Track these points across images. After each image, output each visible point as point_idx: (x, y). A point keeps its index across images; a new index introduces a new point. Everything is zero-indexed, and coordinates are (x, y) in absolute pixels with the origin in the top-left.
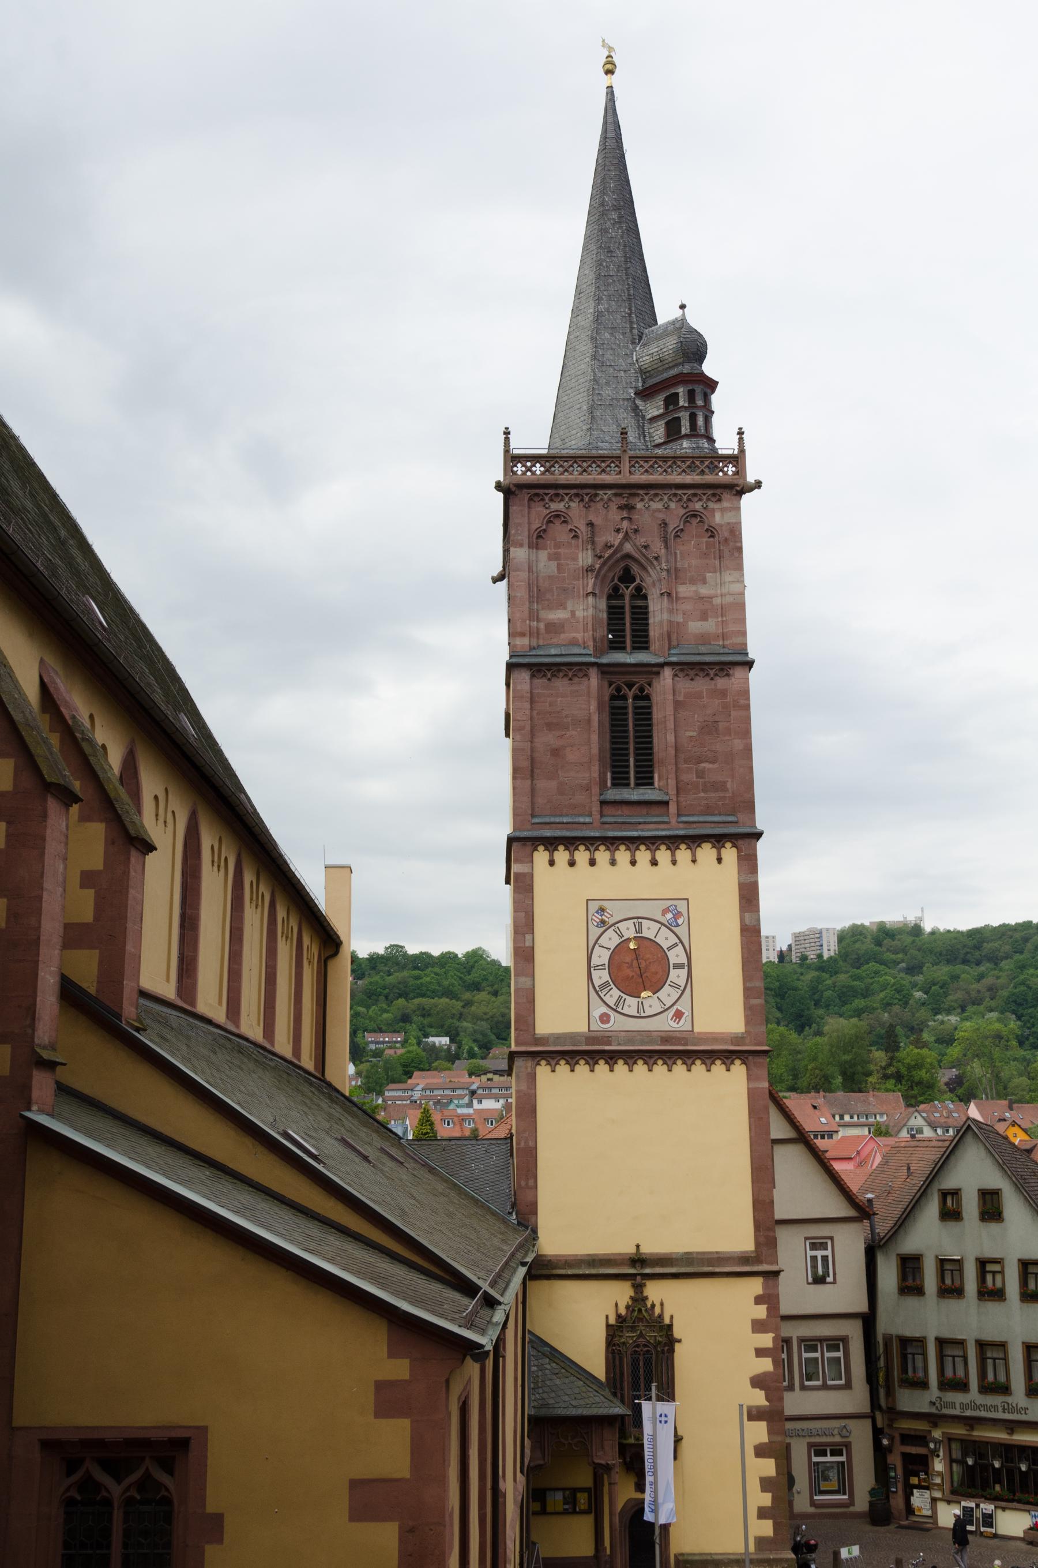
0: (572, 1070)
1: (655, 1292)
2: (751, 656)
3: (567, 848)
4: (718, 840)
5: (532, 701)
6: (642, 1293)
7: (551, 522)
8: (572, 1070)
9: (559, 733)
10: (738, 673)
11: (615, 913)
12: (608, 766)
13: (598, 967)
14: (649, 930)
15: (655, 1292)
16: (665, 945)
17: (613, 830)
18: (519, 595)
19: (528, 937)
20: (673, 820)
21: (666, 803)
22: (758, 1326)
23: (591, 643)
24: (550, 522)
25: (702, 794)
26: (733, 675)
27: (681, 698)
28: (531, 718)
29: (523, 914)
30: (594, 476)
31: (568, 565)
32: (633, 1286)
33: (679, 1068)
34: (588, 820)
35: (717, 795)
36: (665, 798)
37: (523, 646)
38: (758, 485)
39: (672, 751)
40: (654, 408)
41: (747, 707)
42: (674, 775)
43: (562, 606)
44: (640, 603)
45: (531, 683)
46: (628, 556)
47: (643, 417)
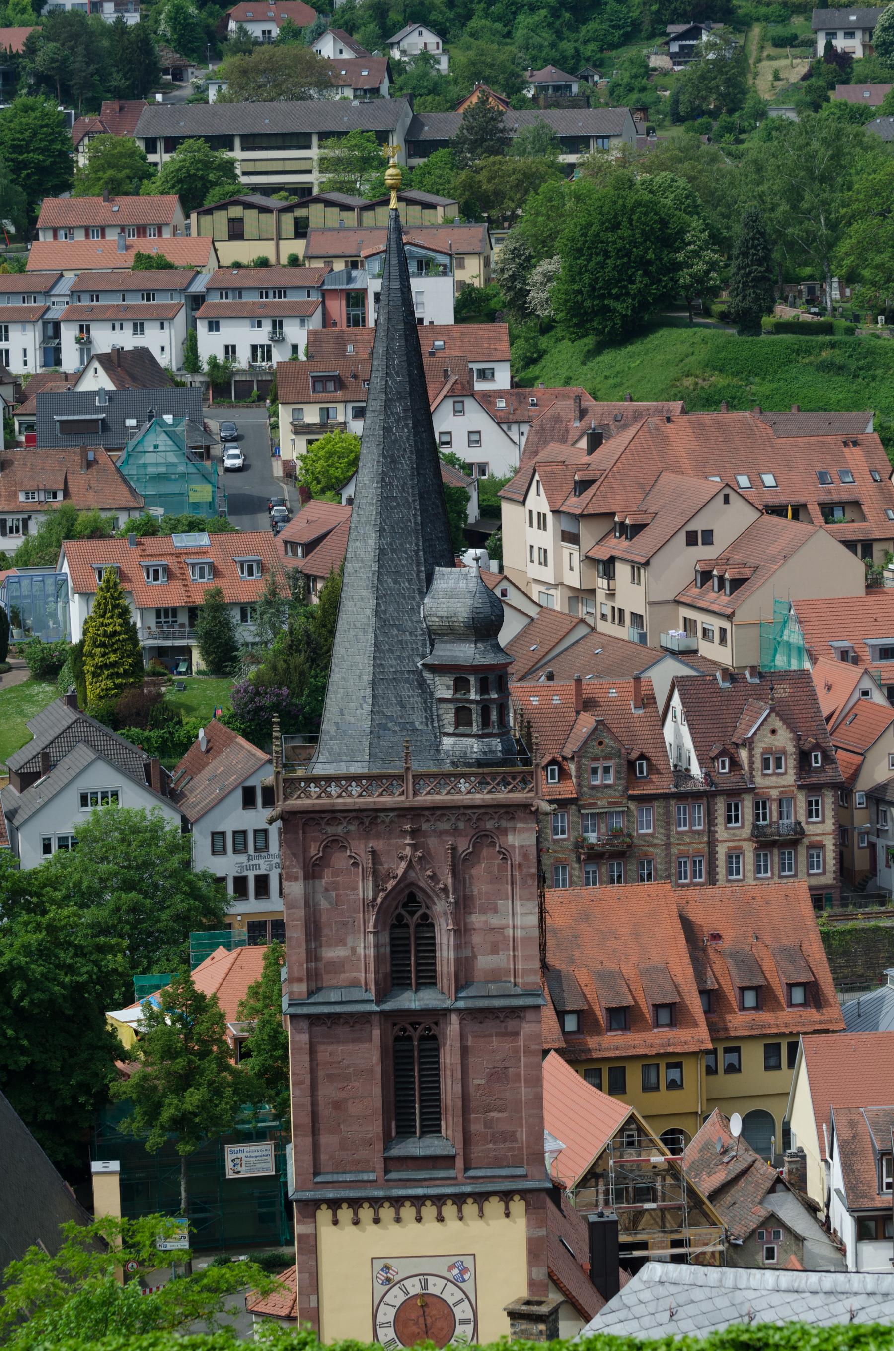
11: (401, 1270)
13: (382, 1325)
14: (435, 1287)
16: (451, 1301)
18: (295, 935)
19: (313, 1298)
26: (524, 1018)
29: (307, 1275)
31: (347, 895)
37: (300, 993)
43: (342, 942)
47: (431, 694)
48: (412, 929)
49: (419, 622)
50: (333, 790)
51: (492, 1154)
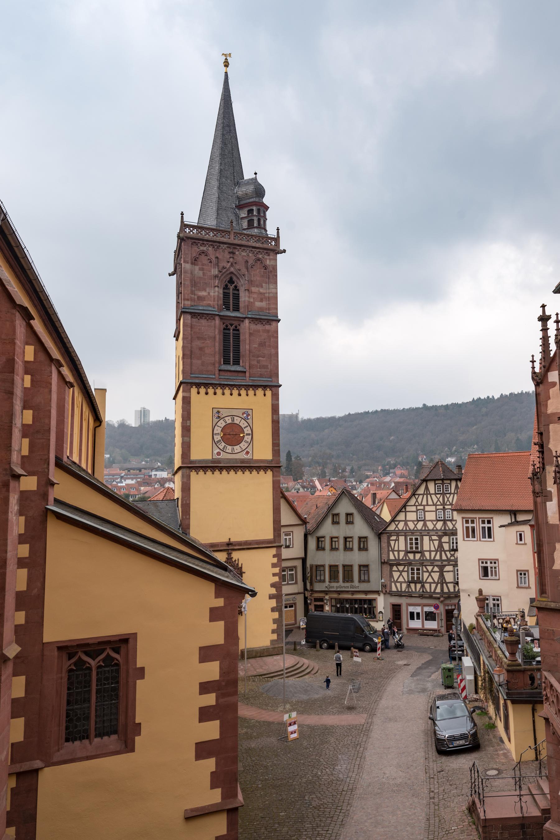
0: (205, 474)
1: (235, 555)
2: (279, 318)
3: (205, 387)
4: (265, 387)
5: (191, 328)
6: (231, 556)
7: (200, 254)
8: (205, 474)
9: (203, 341)
10: (274, 324)
11: (224, 413)
12: (222, 356)
13: (216, 434)
14: (237, 421)
15: (235, 555)
17: (224, 381)
19: (188, 422)
20: (247, 379)
21: (245, 372)
22: (274, 565)
23: (216, 306)
24: (200, 254)
25: (259, 370)
27: (252, 332)
28: (191, 334)
29: (186, 413)
30: (219, 239)
32: (227, 553)
33: (247, 473)
34: (213, 377)
35: (265, 370)
36: (245, 370)
37: (188, 305)
38: (284, 251)
39: (248, 352)
40: (243, 213)
41: (277, 337)
42: (248, 361)
43: (205, 290)
44: (236, 292)
45: (191, 320)
46: (232, 273)
47: (239, 217)
48: (231, 290)
49: (234, 193)
50: (203, 233)
51: (259, 373)
